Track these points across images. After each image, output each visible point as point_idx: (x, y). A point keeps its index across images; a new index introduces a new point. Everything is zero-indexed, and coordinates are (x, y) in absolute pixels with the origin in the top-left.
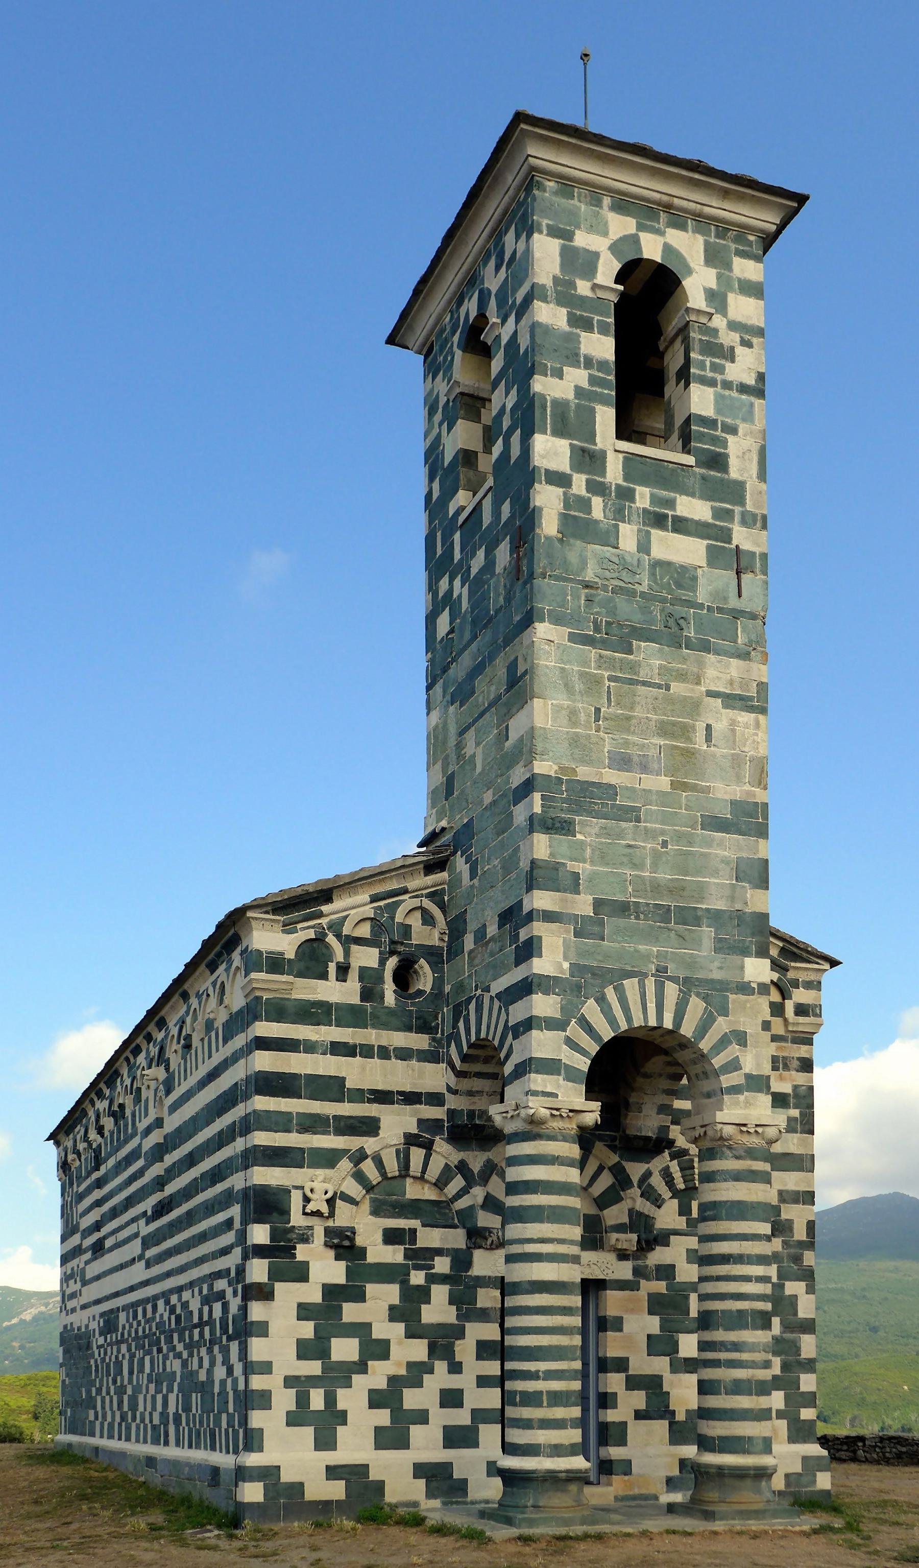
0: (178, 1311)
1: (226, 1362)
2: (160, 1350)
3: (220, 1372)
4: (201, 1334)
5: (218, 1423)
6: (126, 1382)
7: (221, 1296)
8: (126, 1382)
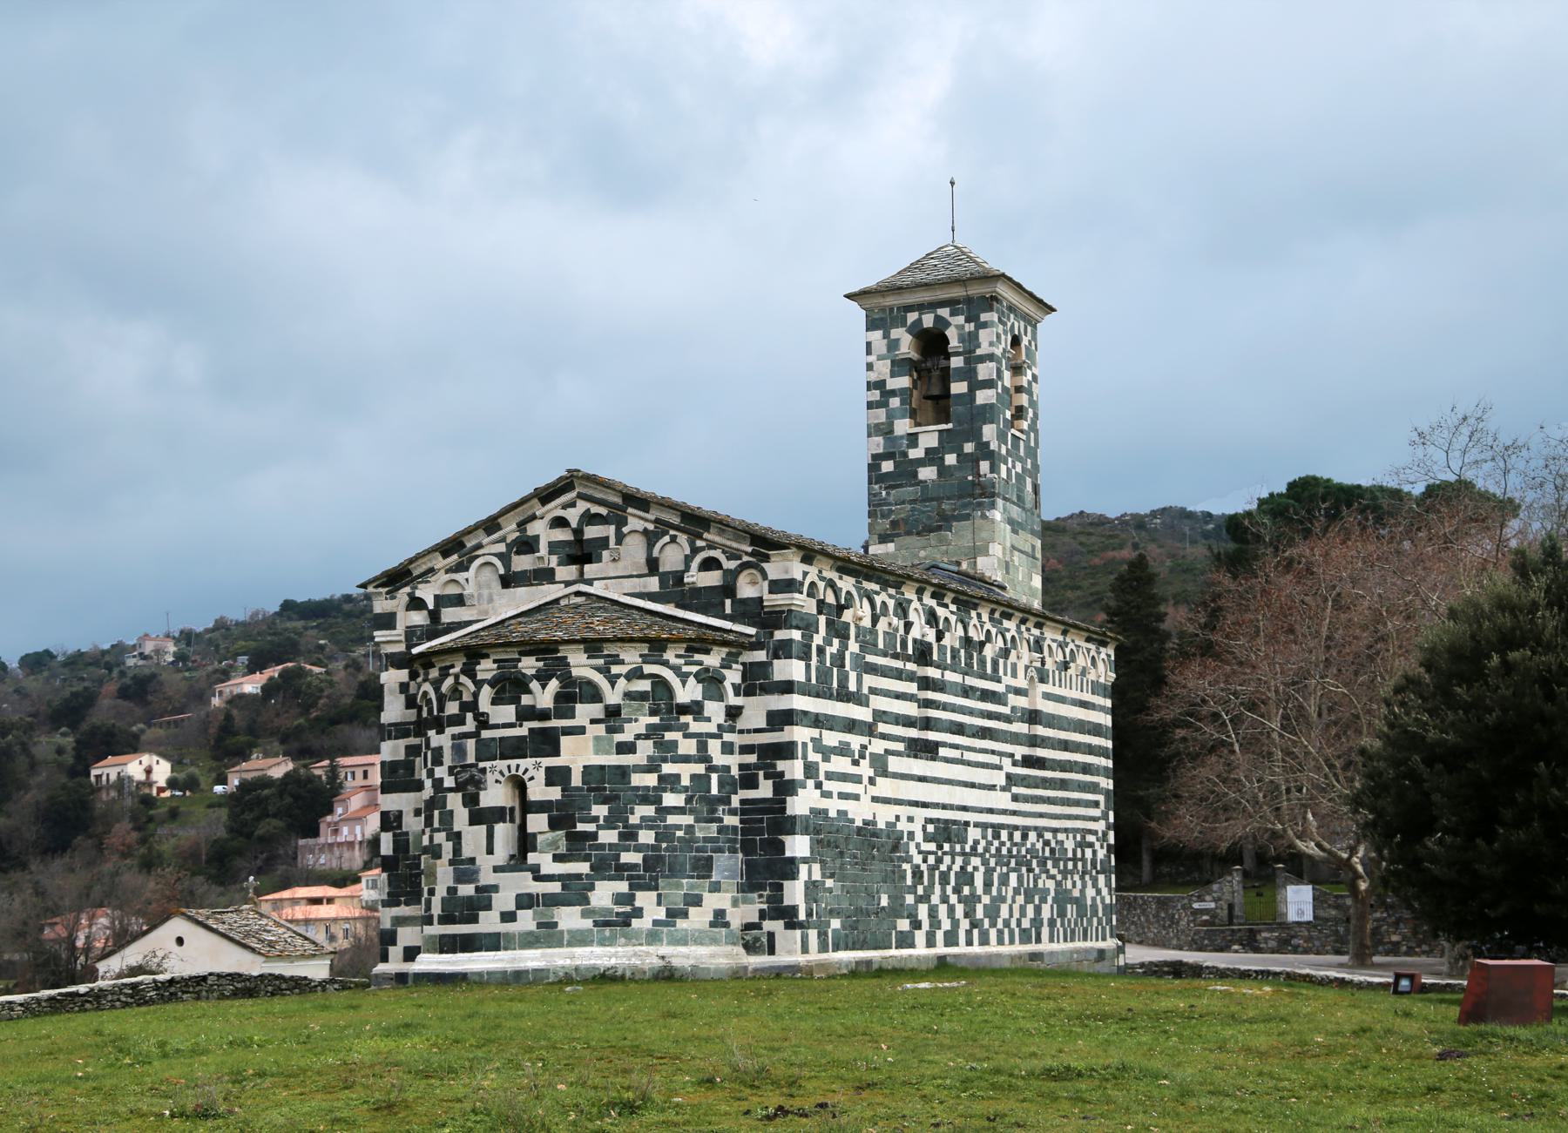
0: (1053, 844)
1: (1095, 885)
2: (1030, 870)
3: (1090, 892)
4: (1075, 866)
5: (1090, 922)
6: (980, 891)
7: (1091, 845)
8: (980, 891)
